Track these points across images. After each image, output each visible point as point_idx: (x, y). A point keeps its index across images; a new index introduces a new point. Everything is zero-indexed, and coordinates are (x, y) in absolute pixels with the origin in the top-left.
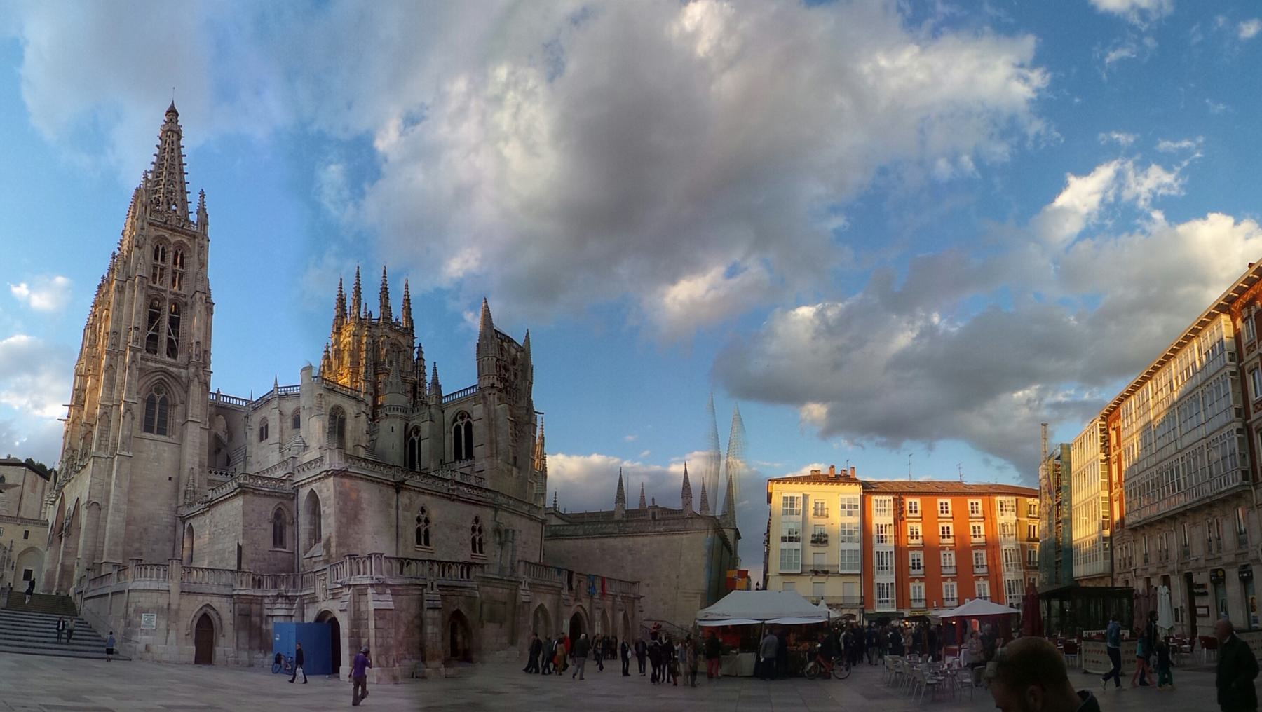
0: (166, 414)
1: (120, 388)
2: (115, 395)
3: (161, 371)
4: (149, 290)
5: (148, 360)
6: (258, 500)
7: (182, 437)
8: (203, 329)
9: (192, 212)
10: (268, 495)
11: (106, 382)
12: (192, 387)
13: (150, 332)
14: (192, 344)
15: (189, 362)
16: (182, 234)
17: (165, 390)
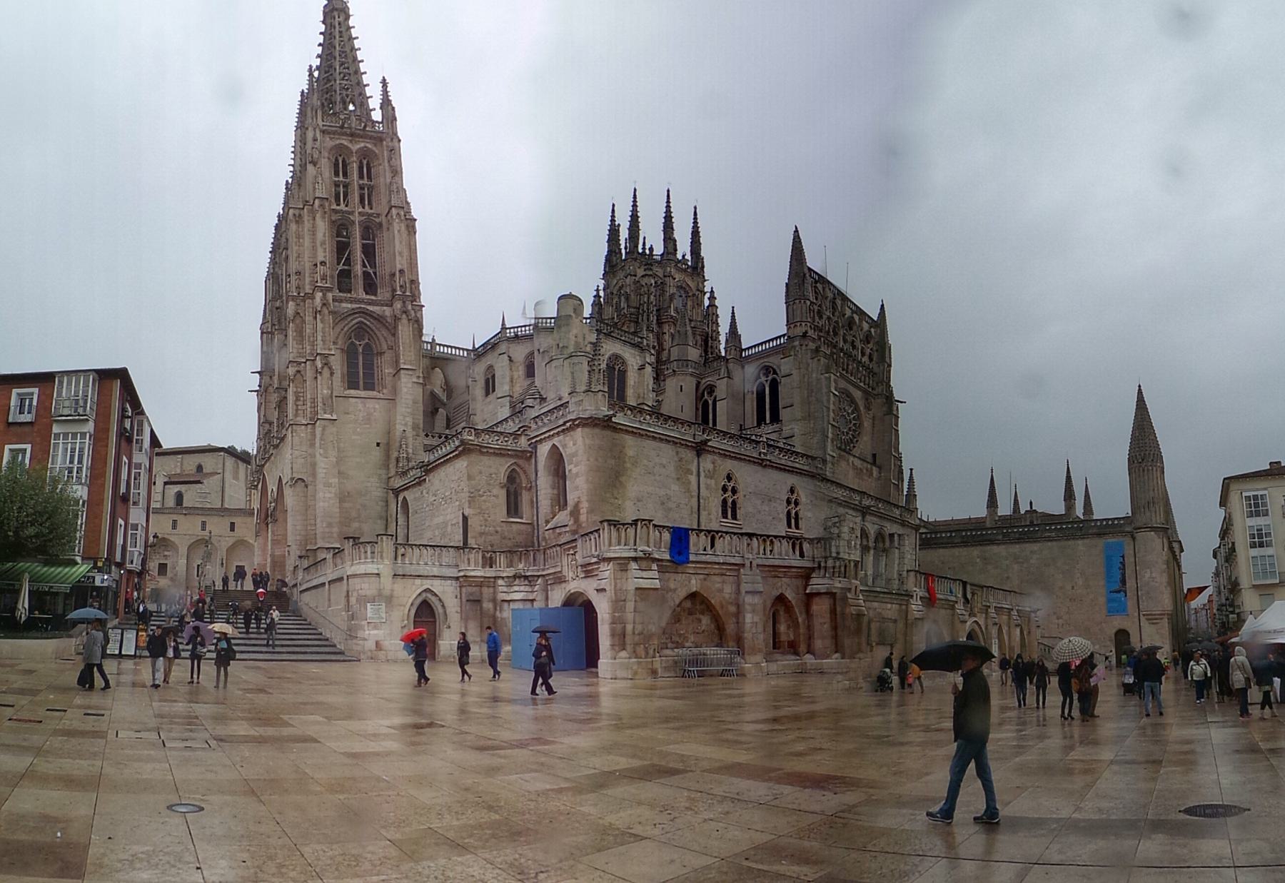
0: (373, 364)
1: (312, 339)
2: (308, 347)
3: (360, 312)
4: (333, 214)
5: (341, 301)
6: (486, 460)
7: (395, 390)
8: (406, 253)
9: (374, 109)
10: (500, 453)
11: (295, 334)
12: (400, 327)
13: (341, 267)
14: (394, 275)
15: (393, 297)
16: (365, 138)
17: (367, 335)
